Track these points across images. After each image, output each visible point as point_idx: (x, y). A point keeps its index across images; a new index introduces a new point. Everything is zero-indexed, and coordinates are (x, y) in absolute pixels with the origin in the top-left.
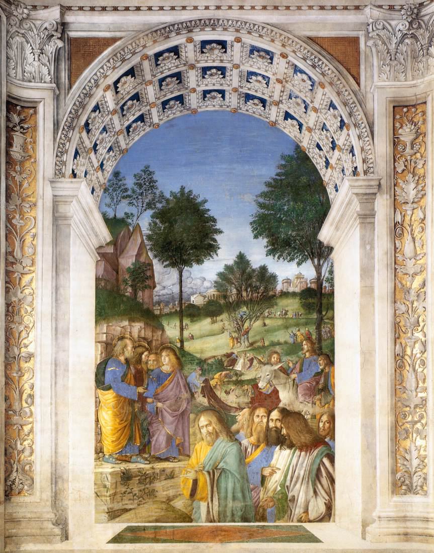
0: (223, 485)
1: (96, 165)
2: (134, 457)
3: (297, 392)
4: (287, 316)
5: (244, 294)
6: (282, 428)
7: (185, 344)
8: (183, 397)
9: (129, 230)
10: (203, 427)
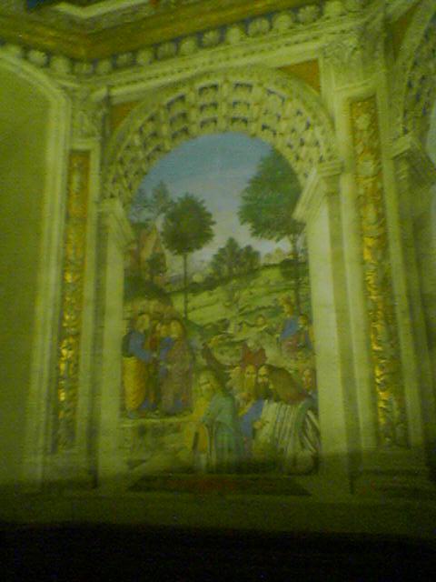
0: (220, 438)
1: (126, 186)
5: (234, 269)
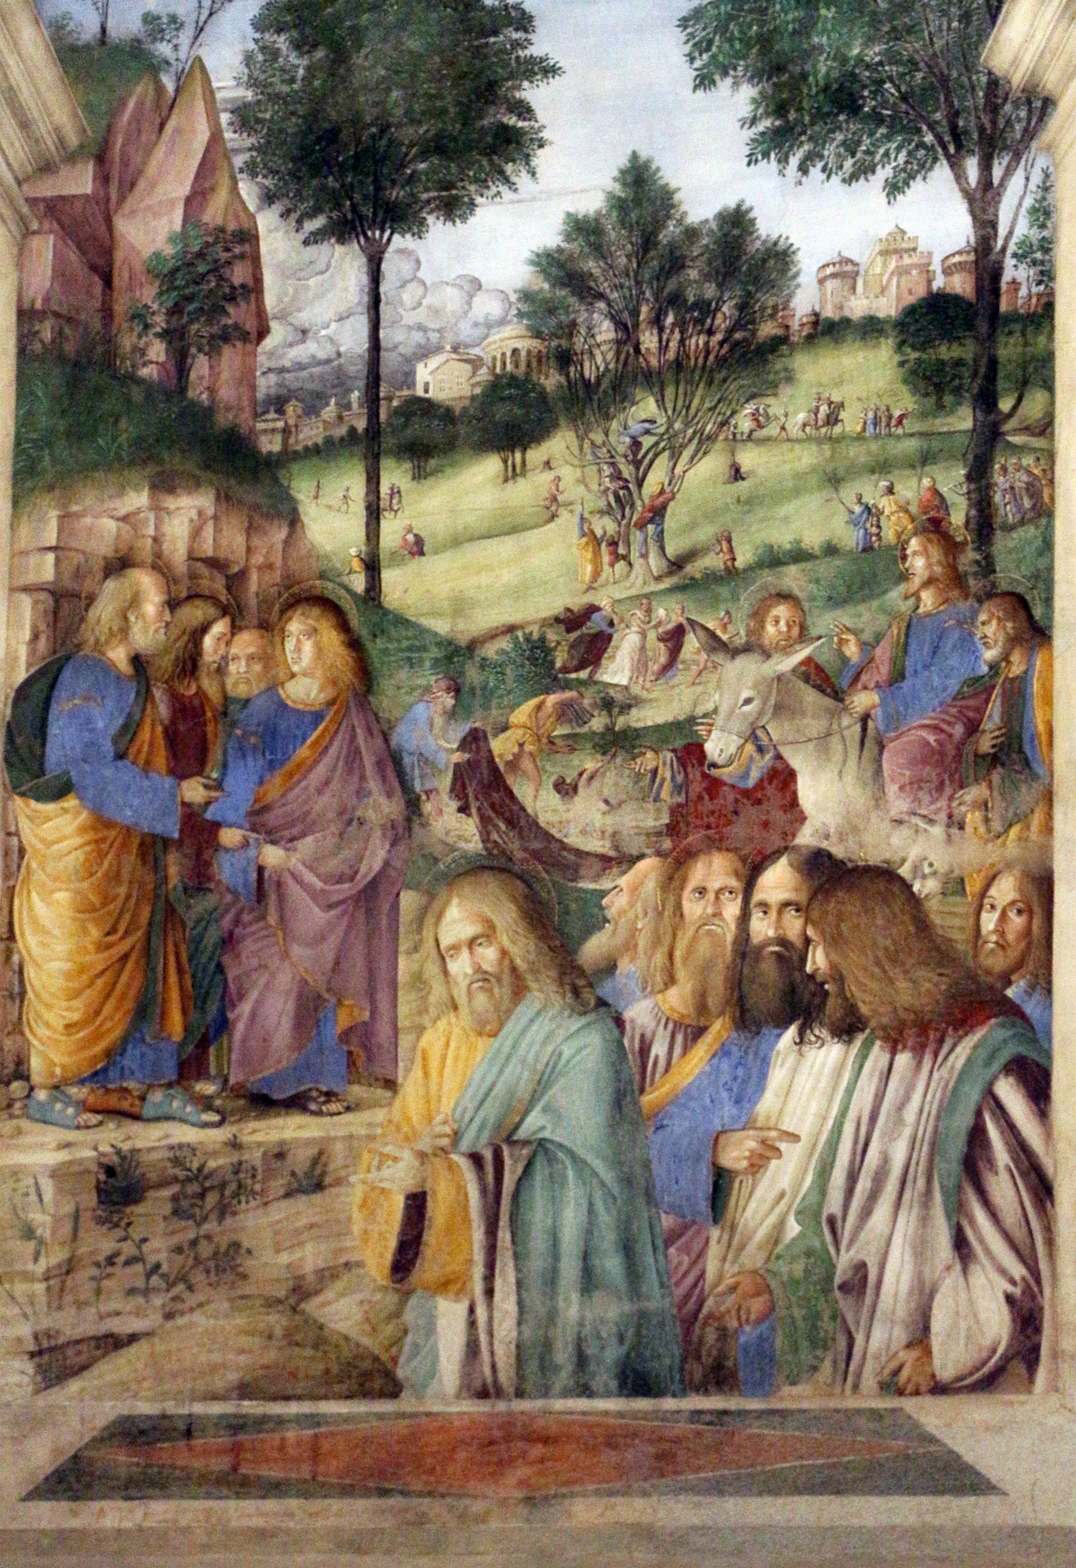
0: (538, 1216)
2: (157, 1096)
3: (878, 772)
4: (838, 429)
5: (649, 340)
6: (807, 941)
7: (389, 576)
8: (371, 815)
9: (160, 88)
10: (455, 947)
